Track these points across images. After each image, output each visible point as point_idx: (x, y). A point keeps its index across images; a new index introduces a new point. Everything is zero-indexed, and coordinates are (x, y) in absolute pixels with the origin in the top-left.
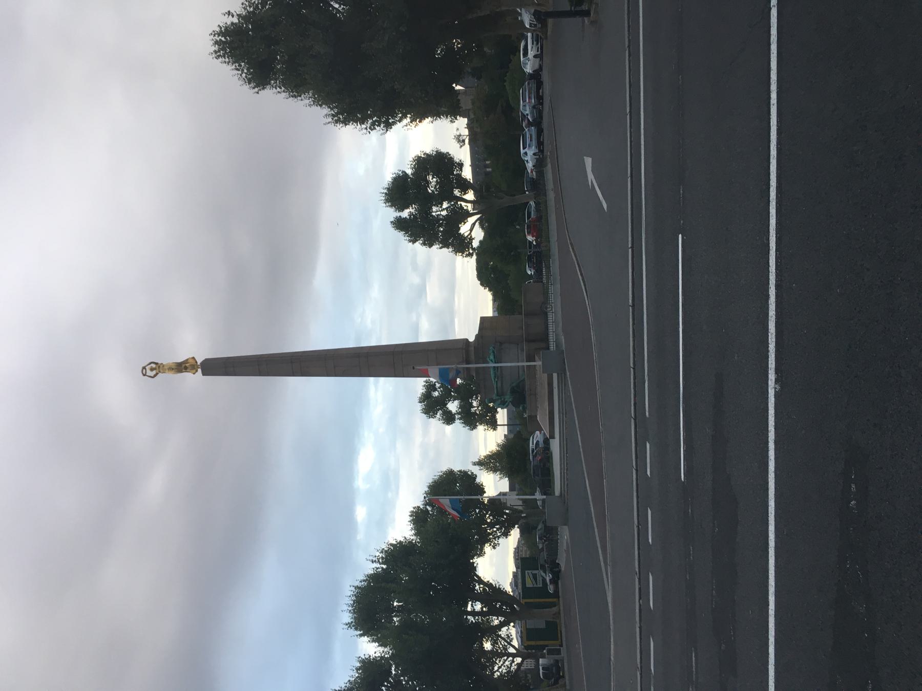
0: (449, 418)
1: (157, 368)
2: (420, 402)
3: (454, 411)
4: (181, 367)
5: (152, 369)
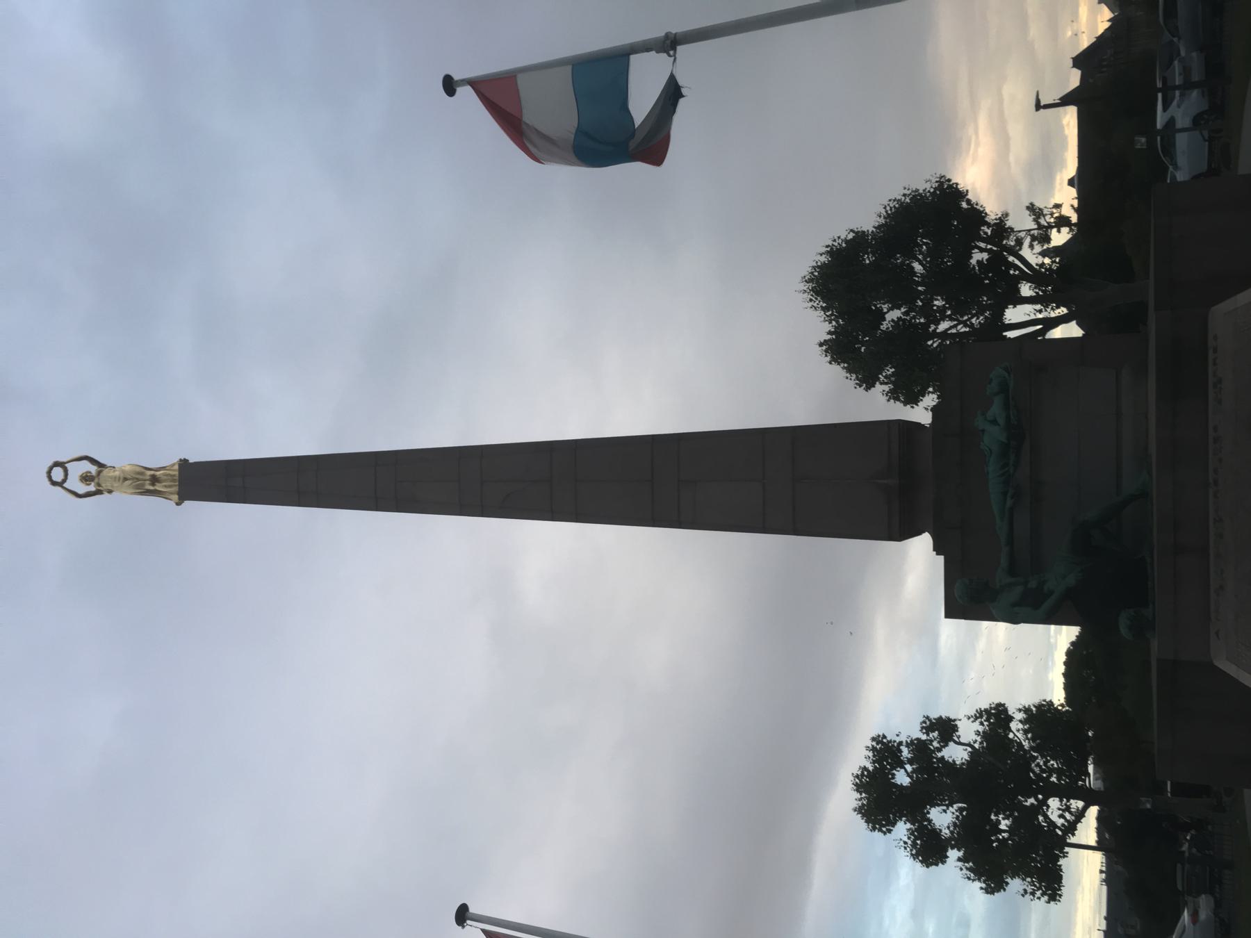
1: (98, 480)
3: (946, 833)
4: (146, 482)
5: (86, 478)
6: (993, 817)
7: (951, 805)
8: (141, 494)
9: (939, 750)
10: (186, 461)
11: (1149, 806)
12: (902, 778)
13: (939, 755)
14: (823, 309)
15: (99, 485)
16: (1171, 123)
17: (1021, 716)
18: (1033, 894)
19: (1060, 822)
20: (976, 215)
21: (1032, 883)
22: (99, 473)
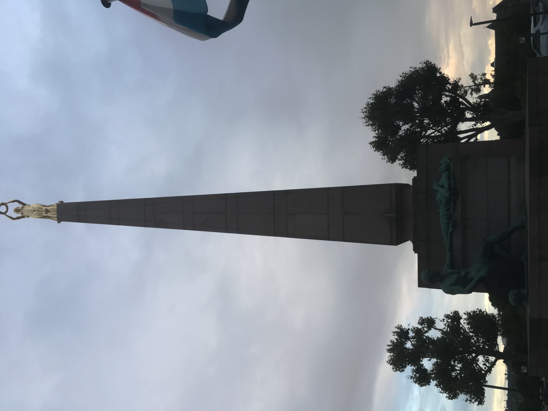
0: (422, 378)
2: (389, 351)
4: (43, 213)
5: (17, 210)
6: (452, 363)
7: (433, 357)
8: (42, 218)
9: (427, 332)
10: (62, 202)
11: (525, 371)
12: (409, 345)
13: (426, 335)
14: (372, 125)
15: (22, 213)
16: (538, 31)
17: (465, 317)
18: (471, 401)
19: (483, 367)
20: (444, 80)
21: (471, 397)
22: (23, 208)
